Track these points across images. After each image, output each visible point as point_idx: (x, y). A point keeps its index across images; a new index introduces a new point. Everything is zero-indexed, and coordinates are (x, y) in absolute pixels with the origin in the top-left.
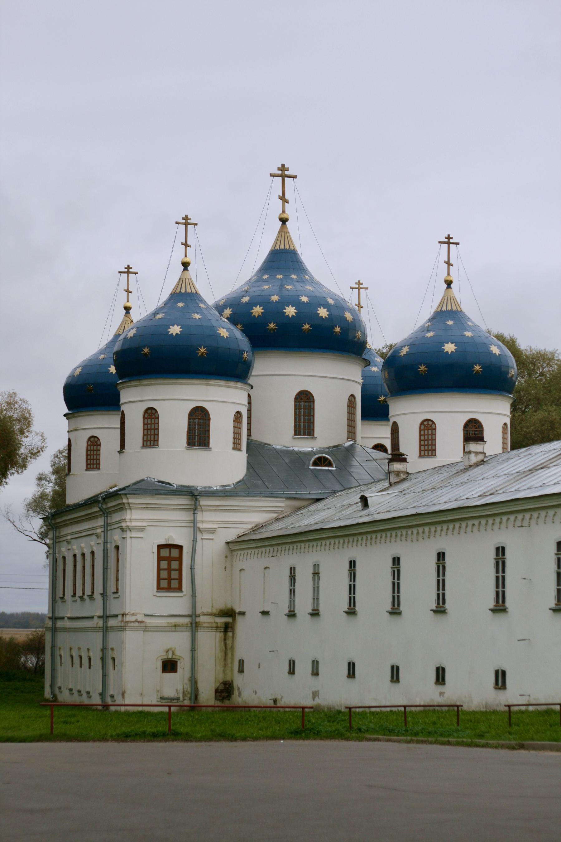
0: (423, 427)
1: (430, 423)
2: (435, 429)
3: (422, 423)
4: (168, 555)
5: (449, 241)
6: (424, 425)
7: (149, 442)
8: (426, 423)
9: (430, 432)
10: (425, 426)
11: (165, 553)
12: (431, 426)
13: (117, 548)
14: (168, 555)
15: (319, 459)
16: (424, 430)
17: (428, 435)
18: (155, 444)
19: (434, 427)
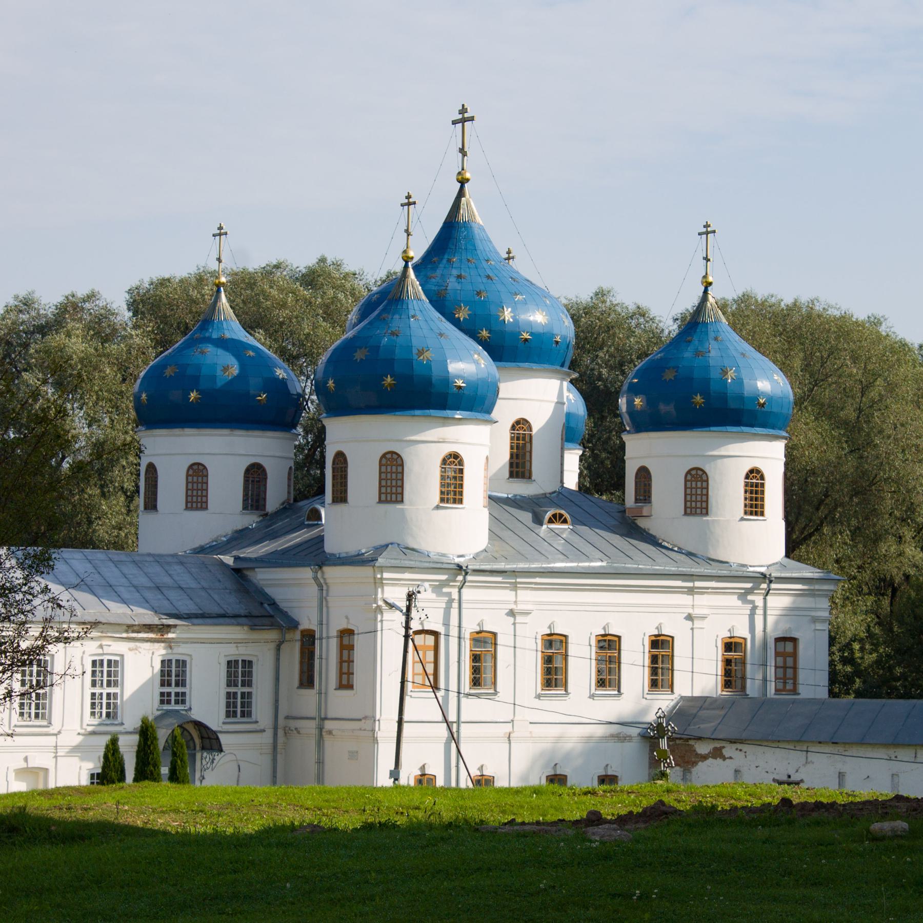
0: (689, 477)
1: (700, 473)
2: (707, 481)
3: (689, 472)
4: (423, 644)
5: (707, 231)
6: (691, 474)
7: (389, 496)
8: (694, 472)
9: (699, 484)
10: (693, 476)
11: (419, 639)
12: (701, 477)
13: (346, 634)
14: (423, 644)
15: (554, 516)
16: (691, 481)
17: (696, 488)
18: (399, 499)
19: (704, 478)
